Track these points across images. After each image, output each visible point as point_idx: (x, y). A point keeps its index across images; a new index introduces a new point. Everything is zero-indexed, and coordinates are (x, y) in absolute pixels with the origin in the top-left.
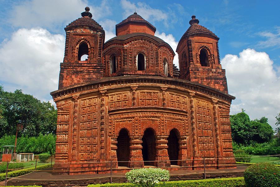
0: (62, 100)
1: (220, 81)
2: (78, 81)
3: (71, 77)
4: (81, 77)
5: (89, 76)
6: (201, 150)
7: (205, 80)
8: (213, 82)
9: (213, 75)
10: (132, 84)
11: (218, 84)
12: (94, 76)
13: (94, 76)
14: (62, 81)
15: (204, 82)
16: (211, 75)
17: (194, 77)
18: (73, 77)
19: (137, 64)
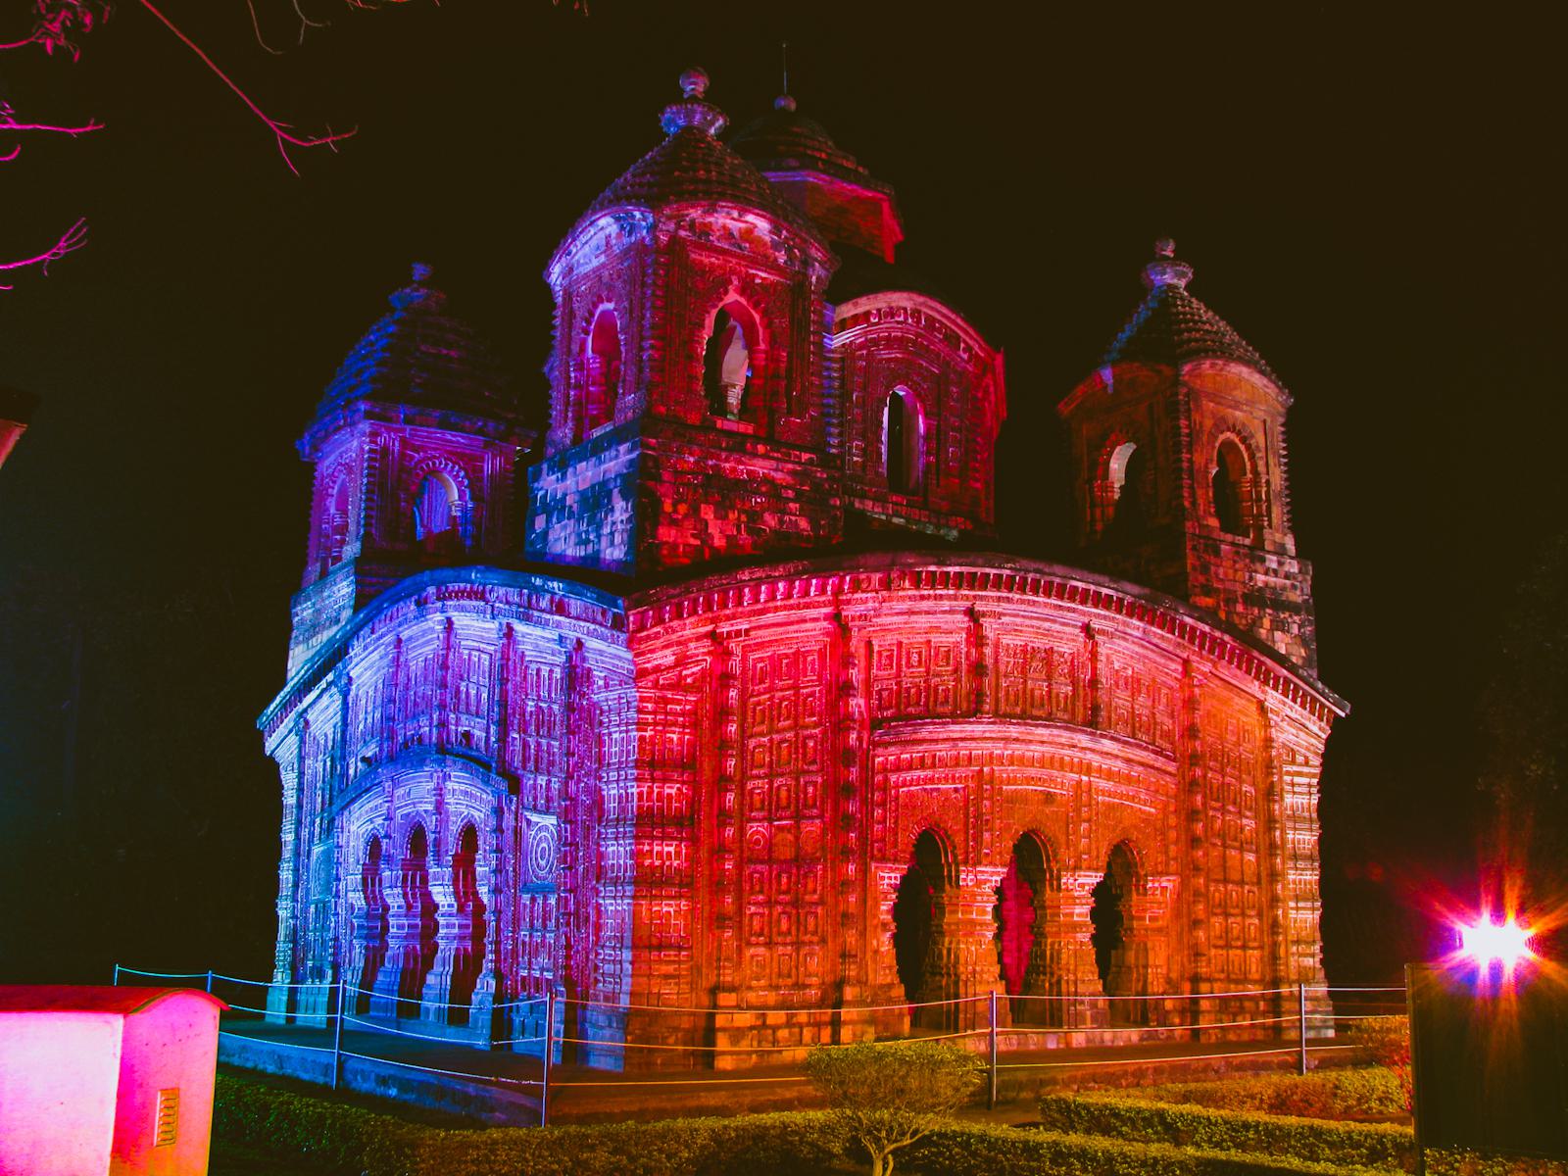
0: (666, 647)
1: (1290, 616)
2: (727, 537)
3: (697, 511)
4: (744, 518)
5: (781, 521)
6: (1216, 947)
7: (1240, 608)
8: (1266, 622)
9: (1266, 584)
10: (982, 598)
11: (1283, 631)
12: (803, 524)
13: (803, 524)
14: (656, 530)
15: (1238, 614)
16: (1260, 584)
17: (1202, 586)
18: (708, 514)
19: (884, 449)
